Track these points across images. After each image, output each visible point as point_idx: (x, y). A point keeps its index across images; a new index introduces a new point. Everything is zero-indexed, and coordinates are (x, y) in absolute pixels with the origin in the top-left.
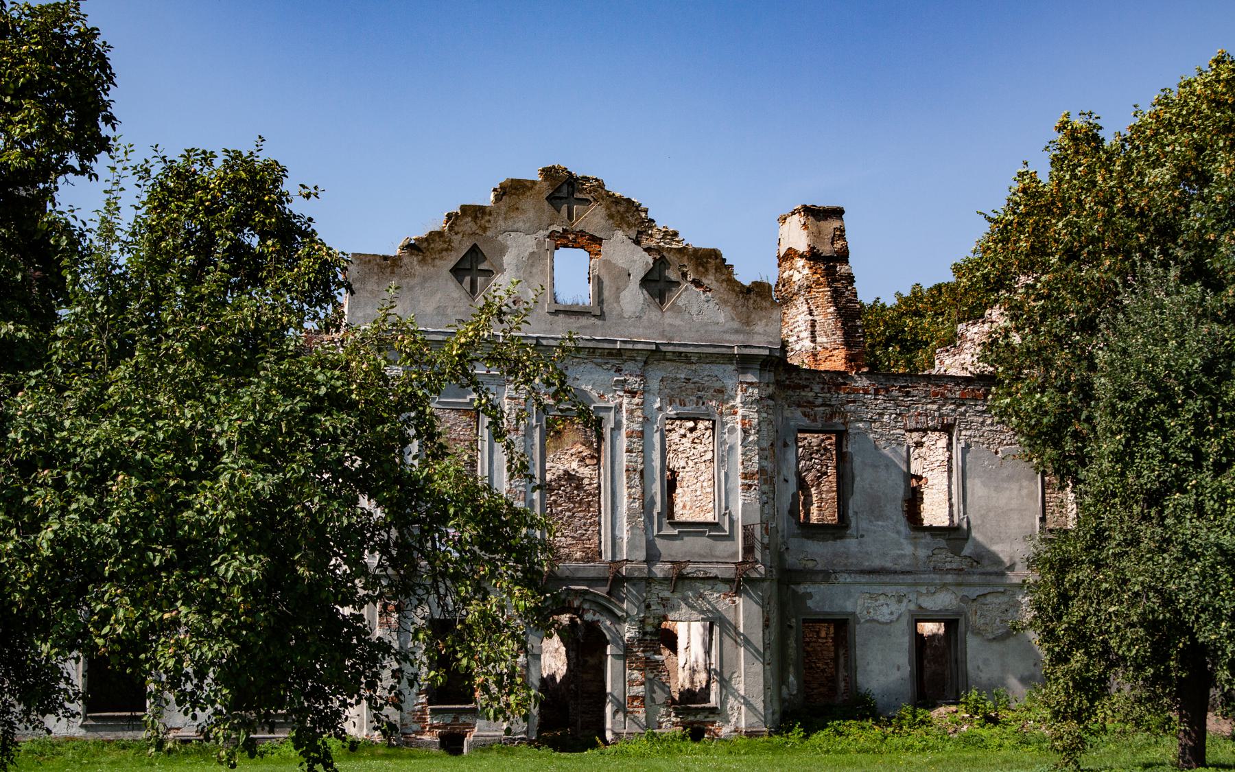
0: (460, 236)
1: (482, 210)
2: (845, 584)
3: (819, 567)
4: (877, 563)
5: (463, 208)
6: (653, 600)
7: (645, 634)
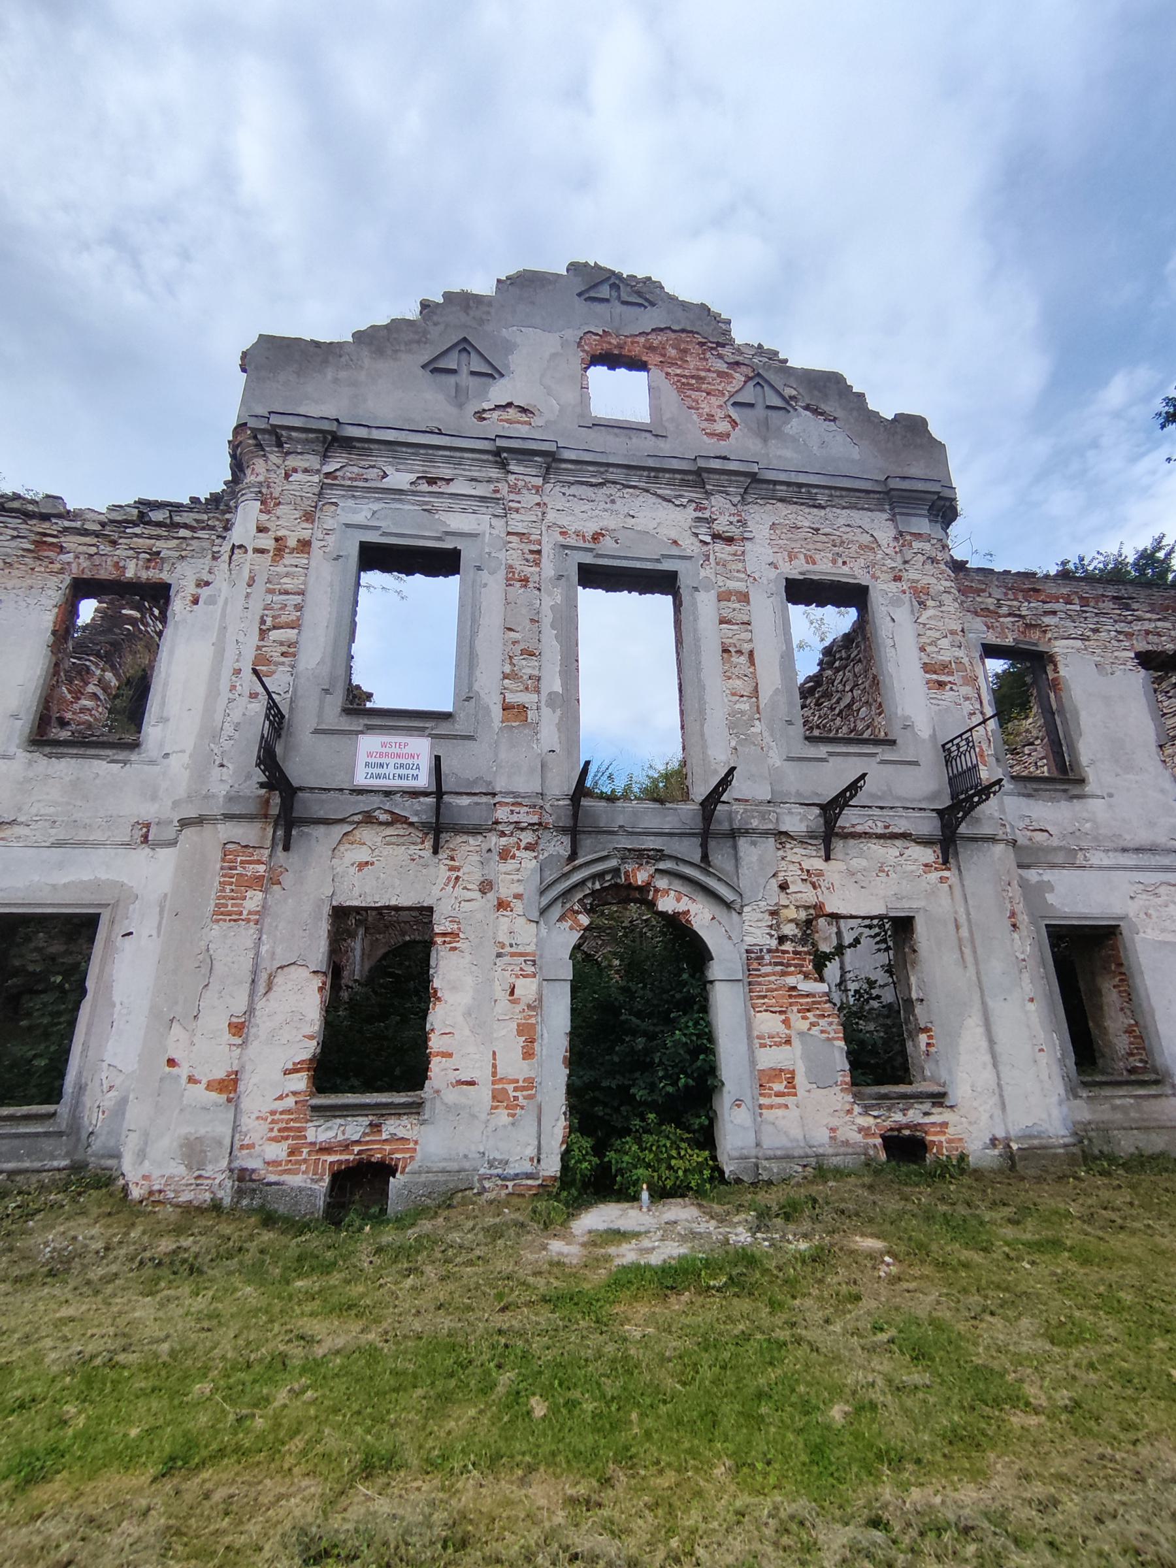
0: (441, 327)
1: (478, 299)
2: (1101, 868)
3: (1055, 842)
4: (1144, 836)
5: (448, 296)
6: (792, 874)
7: (782, 939)
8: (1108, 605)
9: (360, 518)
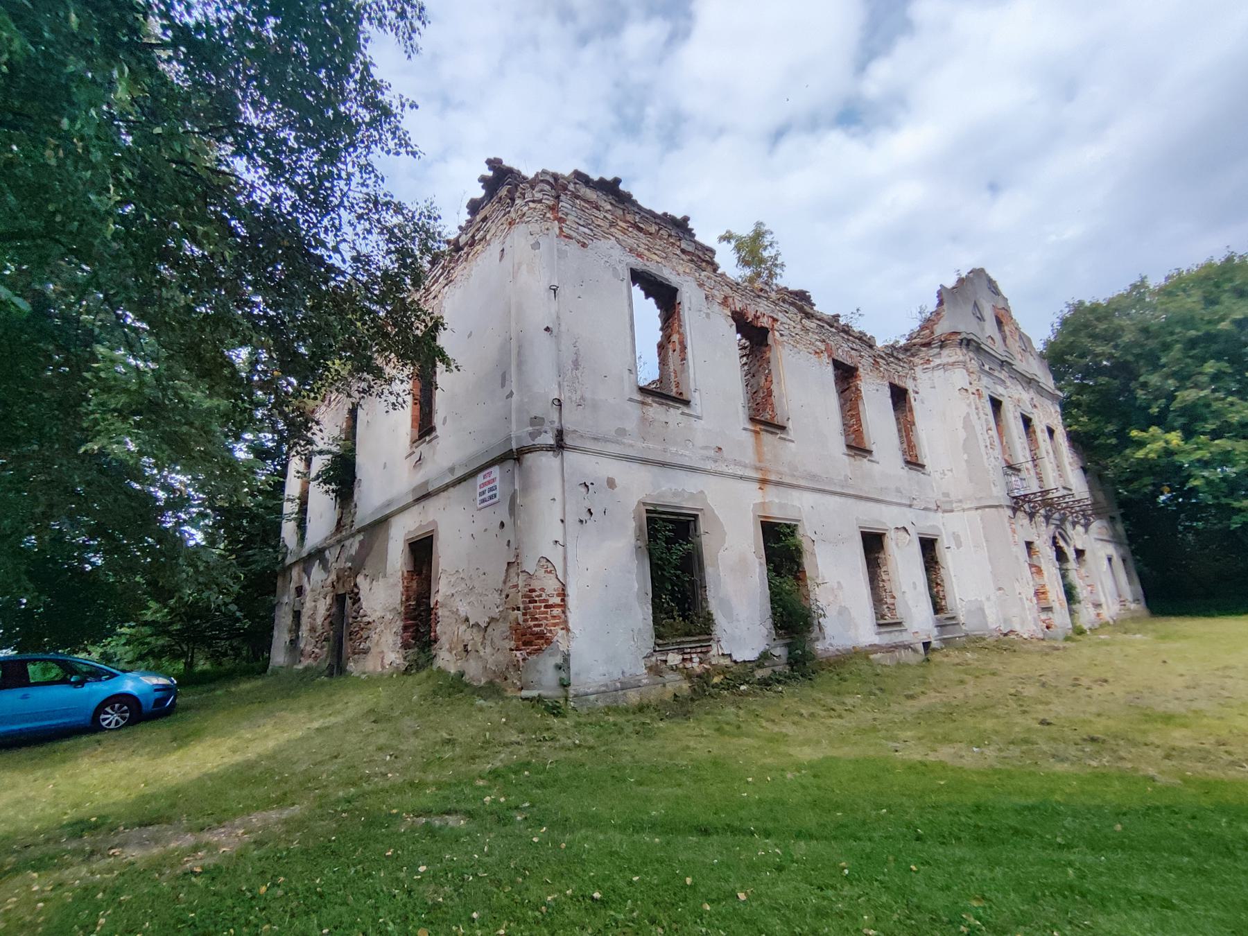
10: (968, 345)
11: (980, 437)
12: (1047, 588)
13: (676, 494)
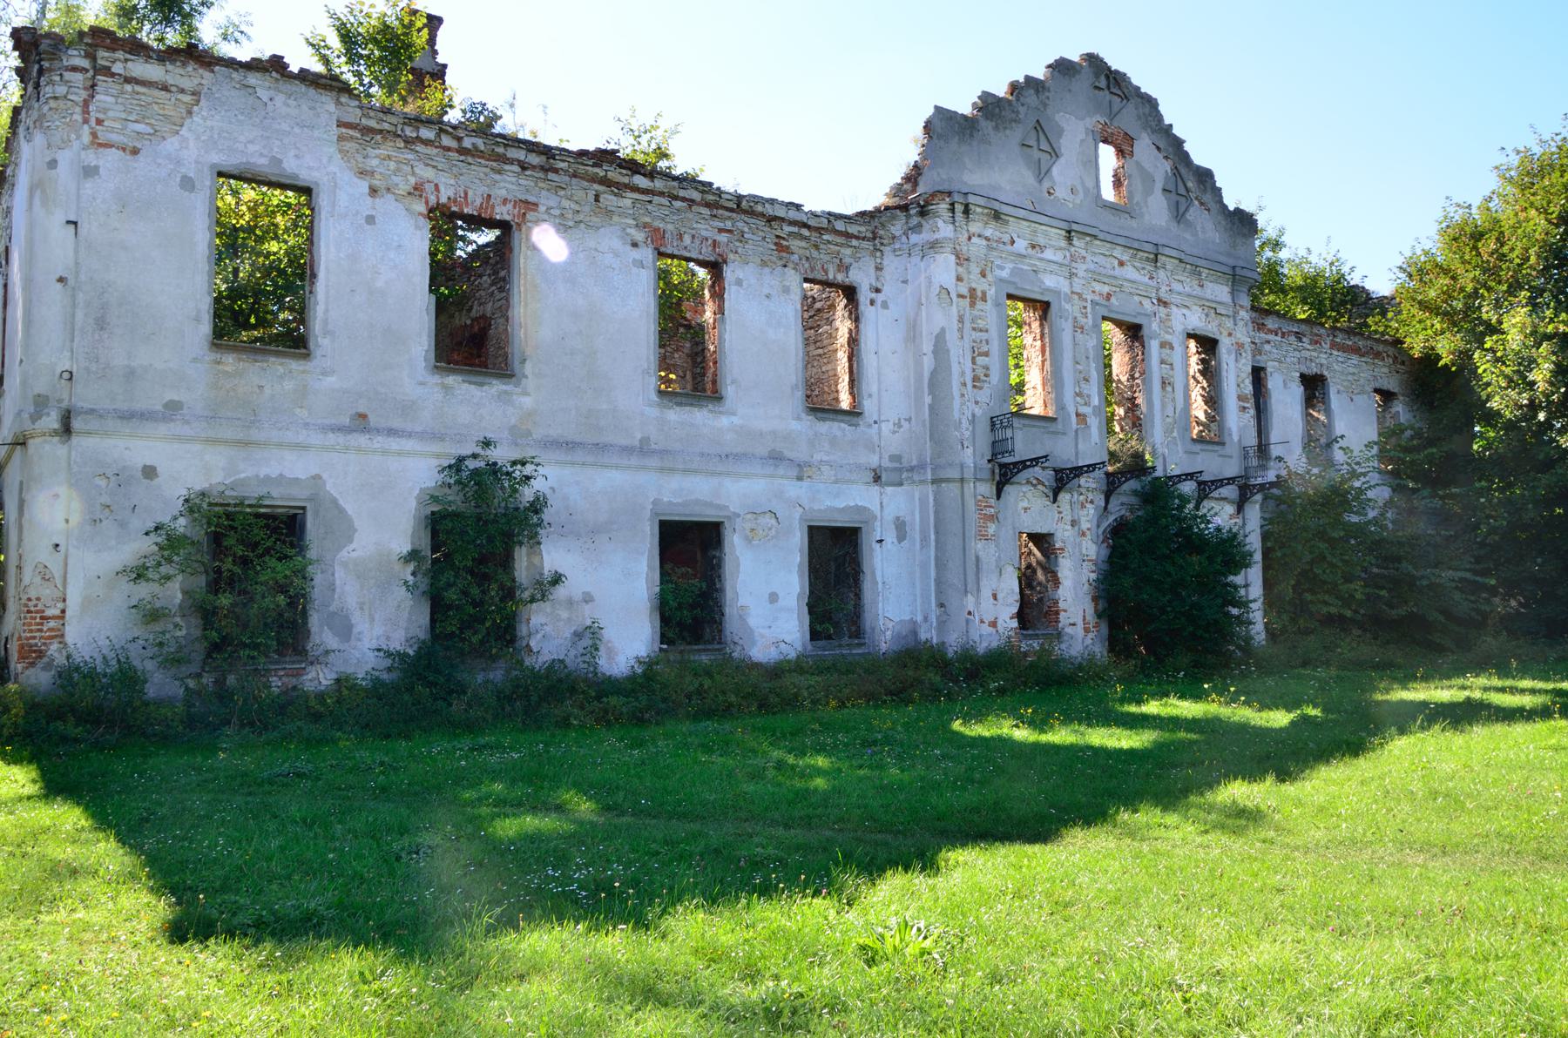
8: (1293, 338)
9: (1004, 274)
10: (966, 211)
11: (955, 369)
12: (1062, 605)
13: (268, 479)
